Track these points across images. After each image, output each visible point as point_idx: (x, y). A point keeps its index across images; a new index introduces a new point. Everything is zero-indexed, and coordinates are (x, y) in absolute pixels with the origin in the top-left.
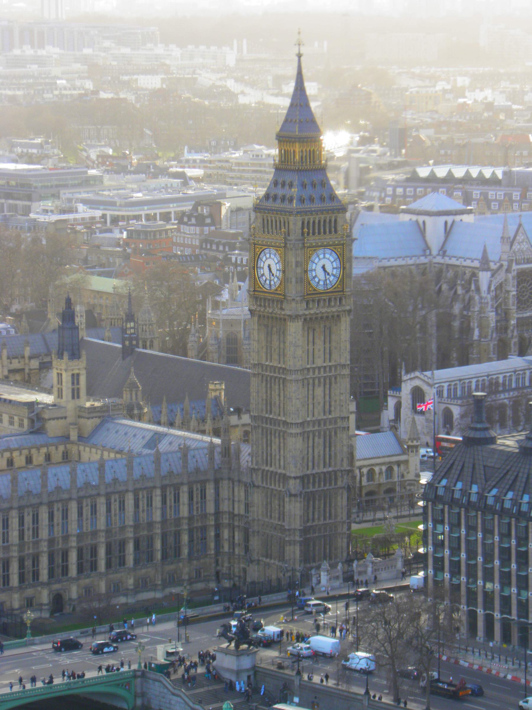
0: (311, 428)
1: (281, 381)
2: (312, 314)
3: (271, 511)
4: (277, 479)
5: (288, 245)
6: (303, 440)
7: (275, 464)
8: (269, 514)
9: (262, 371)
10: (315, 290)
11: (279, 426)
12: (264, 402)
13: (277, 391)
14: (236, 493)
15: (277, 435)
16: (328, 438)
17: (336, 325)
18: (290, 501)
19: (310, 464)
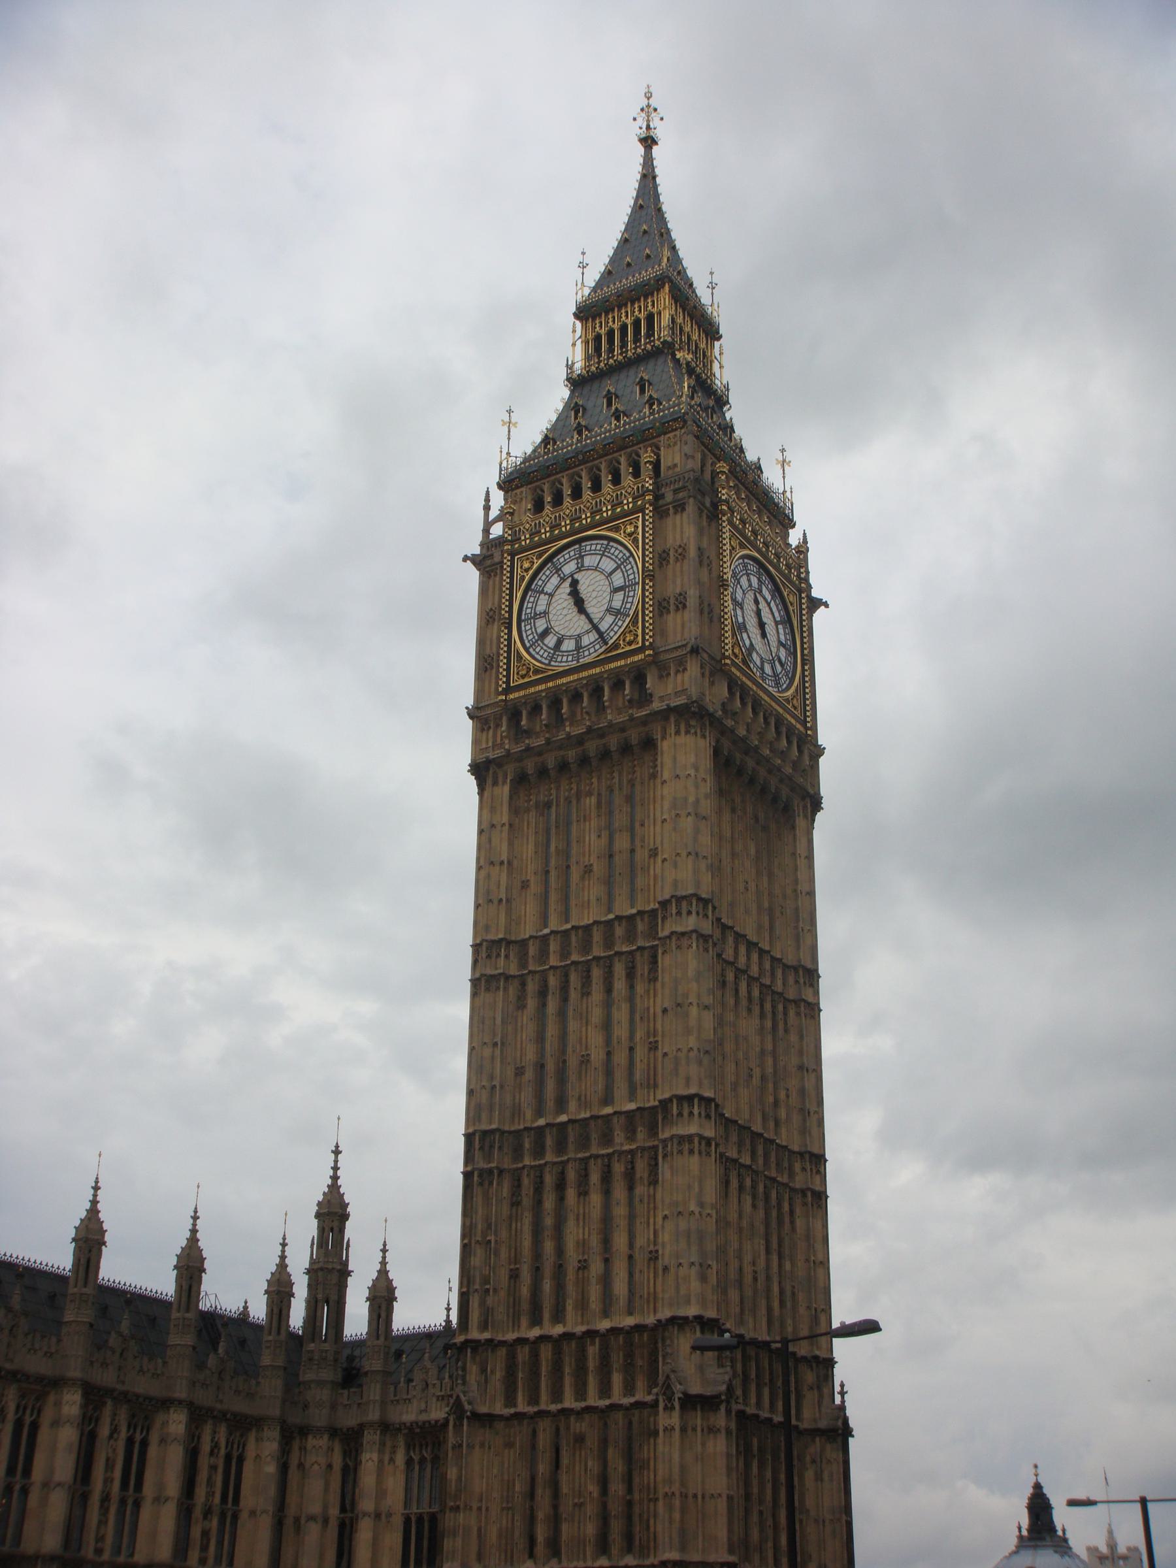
0: (732, 1153)
1: (619, 969)
3: (555, 1520)
4: (592, 1363)
5: (669, 497)
7: (582, 1305)
8: (541, 1533)
9: (523, 964)
10: (744, 662)
11: (607, 1139)
12: (529, 1074)
13: (597, 1015)
14: (367, 1479)
15: (595, 1178)
18: (683, 1430)
19: (734, 1295)
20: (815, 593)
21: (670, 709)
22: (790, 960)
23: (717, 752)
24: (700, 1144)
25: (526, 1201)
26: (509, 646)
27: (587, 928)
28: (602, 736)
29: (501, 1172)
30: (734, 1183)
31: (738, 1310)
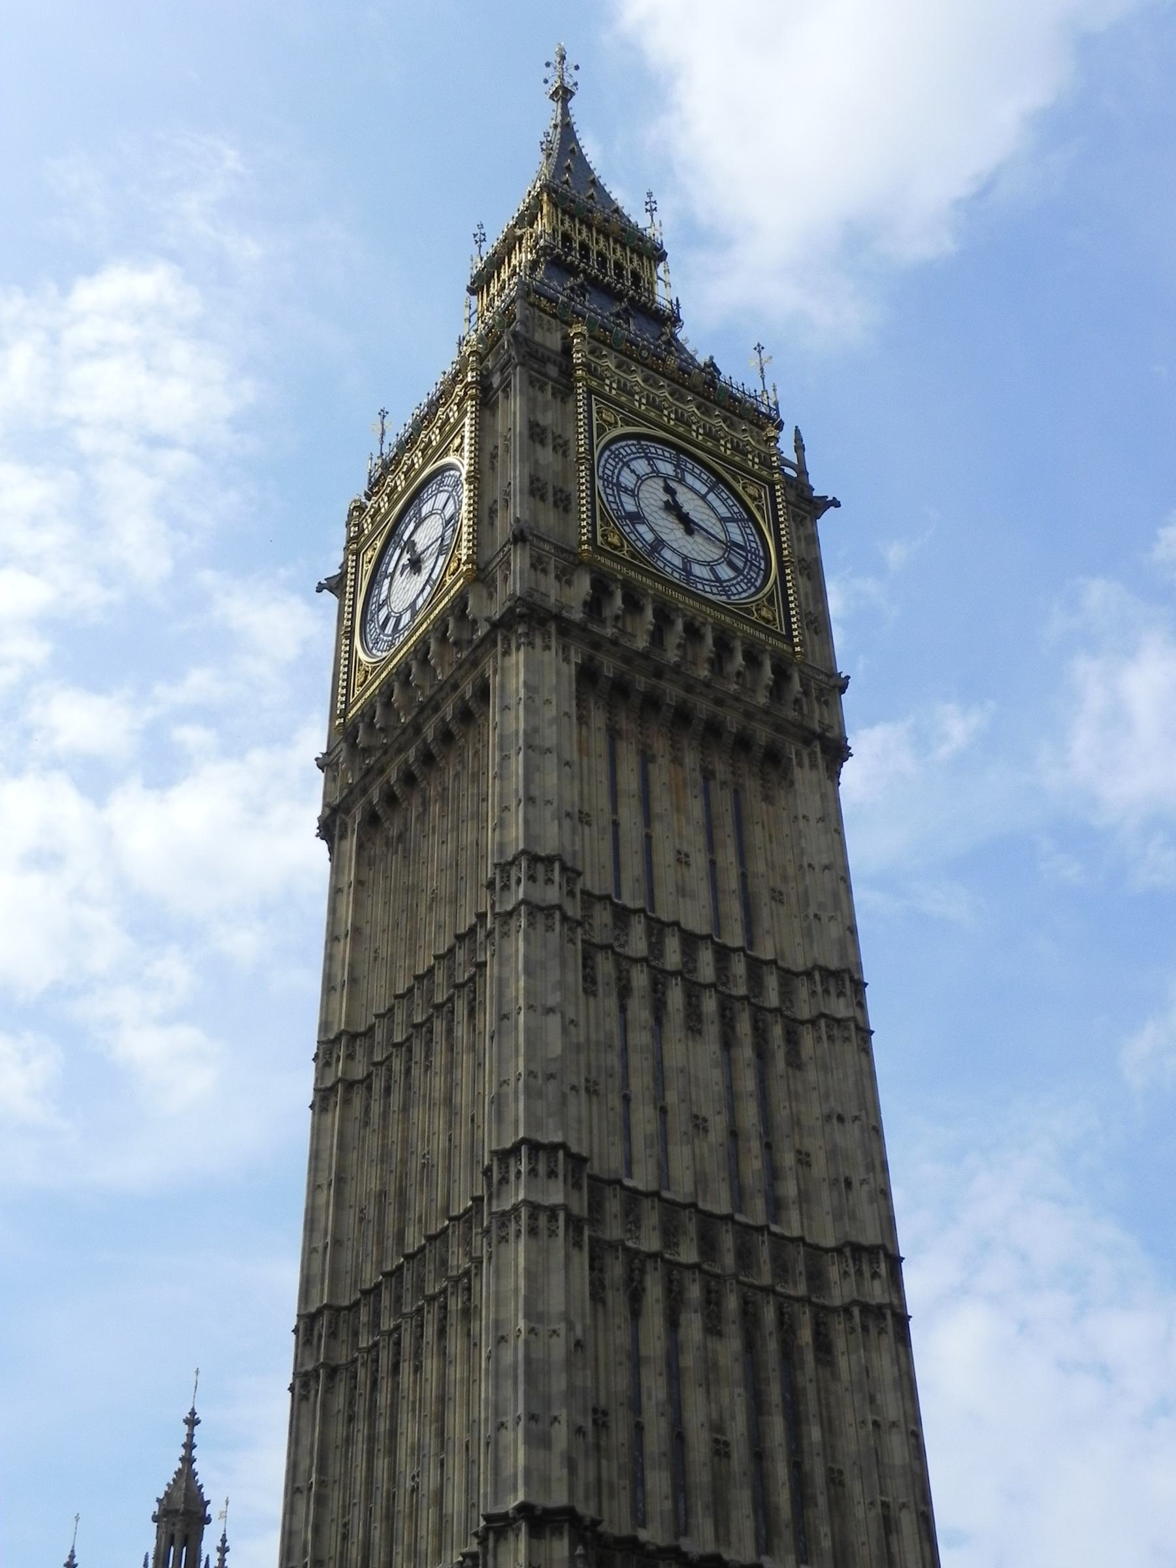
0: (650, 1242)
2: (629, 657)
5: (496, 380)
6: (597, 1294)
12: (371, 1212)
15: (430, 1332)
16: (772, 1345)
17: (768, 799)
19: (658, 1482)
20: (815, 494)
21: (495, 626)
22: (797, 961)
23: (587, 675)
24: (533, 1217)
25: (361, 1407)
26: (349, 659)
27: (431, 971)
28: (436, 709)
29: (333, 1372)
30: (654, 1290)
31: (668, 1505)
